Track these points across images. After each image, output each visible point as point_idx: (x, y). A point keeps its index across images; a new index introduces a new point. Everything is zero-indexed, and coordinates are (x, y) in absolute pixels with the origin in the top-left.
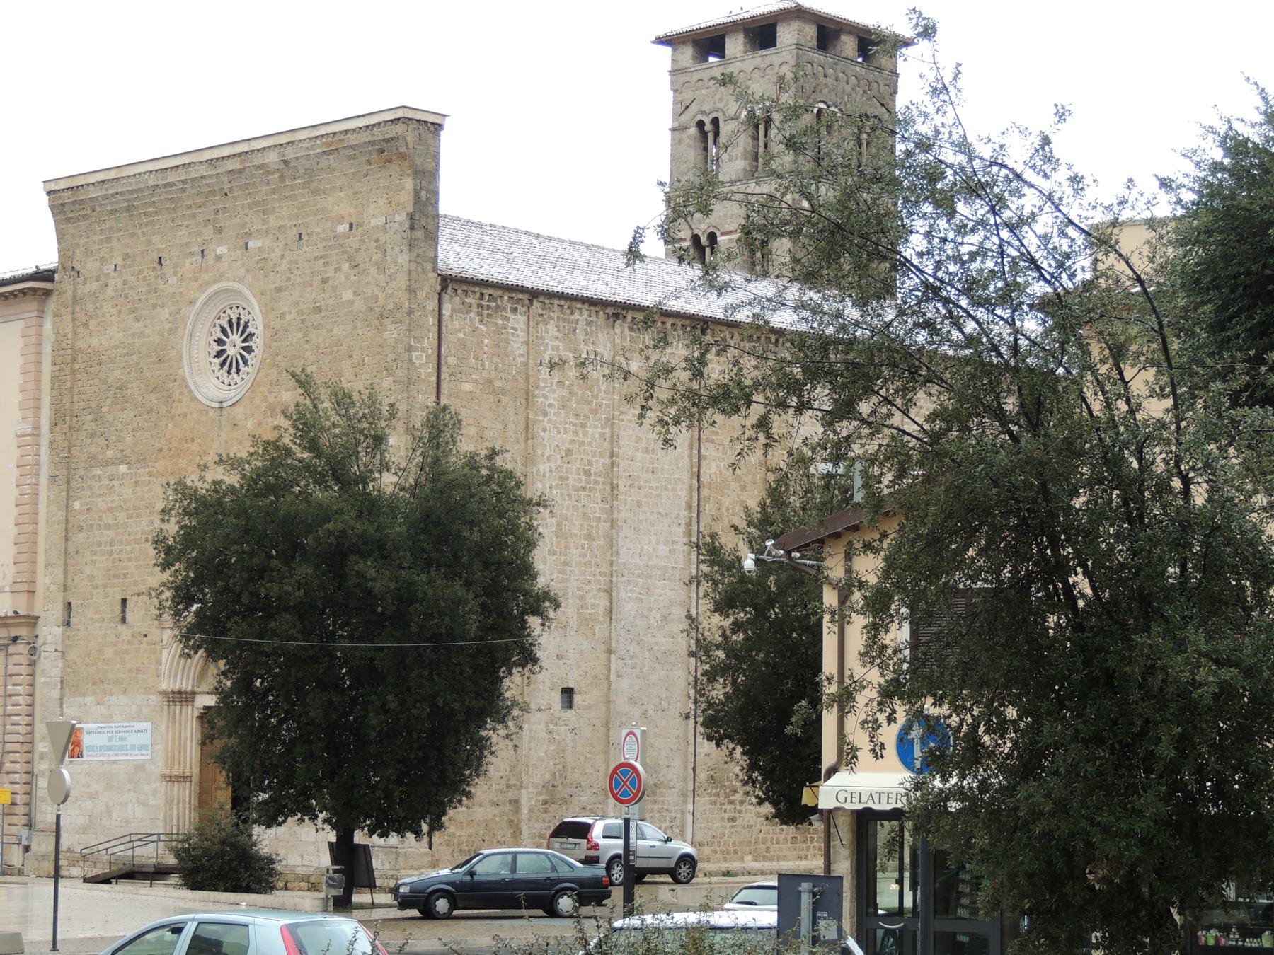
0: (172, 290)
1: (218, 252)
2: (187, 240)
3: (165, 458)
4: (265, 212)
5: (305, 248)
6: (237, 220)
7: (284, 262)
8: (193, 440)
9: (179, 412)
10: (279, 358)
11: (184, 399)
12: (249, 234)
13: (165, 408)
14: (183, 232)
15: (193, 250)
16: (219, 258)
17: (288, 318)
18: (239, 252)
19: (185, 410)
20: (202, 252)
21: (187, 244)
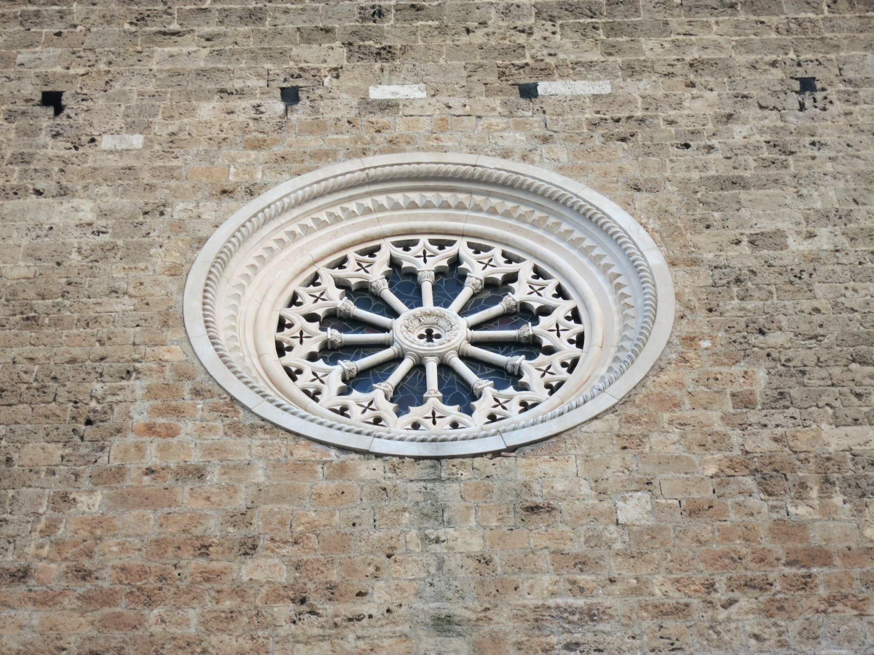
0: (114, 162)
1: (377, 93)
2: (202, 64)
3: (47, 601)
4: (613, 29)
5: (838, 107)
6: (478, 37)
7: (738, 132)
8: (249, 548)
9: (152, 458)
10: (775, 338)
11: (187, 427)
12: (547, 72)
13: (57, 451)
14: (188, 45)
15: (238, 84)
16: (387, 106)
17: (797, 245)
18: (496, 102)
19: (195, 458)
20: (290, 96)
21: (201, 73)
